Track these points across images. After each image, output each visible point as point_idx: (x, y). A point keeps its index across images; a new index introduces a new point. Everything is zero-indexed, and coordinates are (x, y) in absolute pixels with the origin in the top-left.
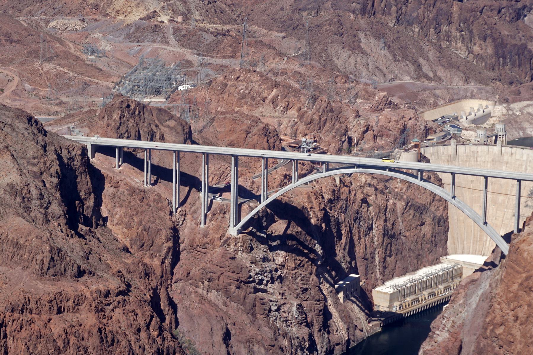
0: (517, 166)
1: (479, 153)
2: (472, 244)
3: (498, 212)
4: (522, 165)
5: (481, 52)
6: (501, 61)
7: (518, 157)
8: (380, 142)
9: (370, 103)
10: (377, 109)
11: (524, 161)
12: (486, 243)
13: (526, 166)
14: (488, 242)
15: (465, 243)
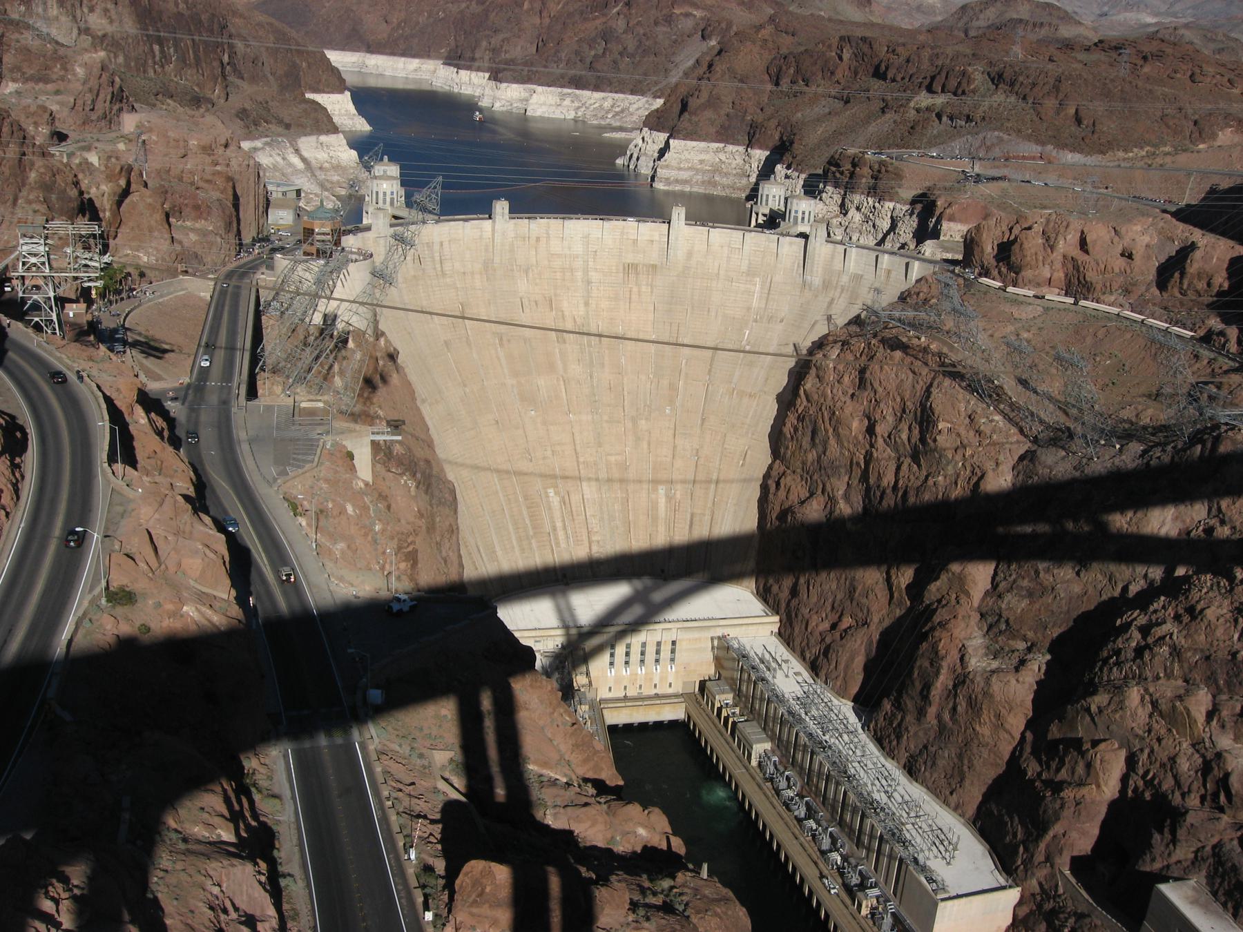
0: (559, 275)
1: (446, 245)
2: (517, 550)
4: (572, 270)
5: (110, 29)
6: (157, 53)
7: (556, 246)
8: (191, 231)
9: (57, 92)
10: (94, 117)
12: (556, 539)
13: (586, 271)
14: (561, 534)
15: (499, 553)
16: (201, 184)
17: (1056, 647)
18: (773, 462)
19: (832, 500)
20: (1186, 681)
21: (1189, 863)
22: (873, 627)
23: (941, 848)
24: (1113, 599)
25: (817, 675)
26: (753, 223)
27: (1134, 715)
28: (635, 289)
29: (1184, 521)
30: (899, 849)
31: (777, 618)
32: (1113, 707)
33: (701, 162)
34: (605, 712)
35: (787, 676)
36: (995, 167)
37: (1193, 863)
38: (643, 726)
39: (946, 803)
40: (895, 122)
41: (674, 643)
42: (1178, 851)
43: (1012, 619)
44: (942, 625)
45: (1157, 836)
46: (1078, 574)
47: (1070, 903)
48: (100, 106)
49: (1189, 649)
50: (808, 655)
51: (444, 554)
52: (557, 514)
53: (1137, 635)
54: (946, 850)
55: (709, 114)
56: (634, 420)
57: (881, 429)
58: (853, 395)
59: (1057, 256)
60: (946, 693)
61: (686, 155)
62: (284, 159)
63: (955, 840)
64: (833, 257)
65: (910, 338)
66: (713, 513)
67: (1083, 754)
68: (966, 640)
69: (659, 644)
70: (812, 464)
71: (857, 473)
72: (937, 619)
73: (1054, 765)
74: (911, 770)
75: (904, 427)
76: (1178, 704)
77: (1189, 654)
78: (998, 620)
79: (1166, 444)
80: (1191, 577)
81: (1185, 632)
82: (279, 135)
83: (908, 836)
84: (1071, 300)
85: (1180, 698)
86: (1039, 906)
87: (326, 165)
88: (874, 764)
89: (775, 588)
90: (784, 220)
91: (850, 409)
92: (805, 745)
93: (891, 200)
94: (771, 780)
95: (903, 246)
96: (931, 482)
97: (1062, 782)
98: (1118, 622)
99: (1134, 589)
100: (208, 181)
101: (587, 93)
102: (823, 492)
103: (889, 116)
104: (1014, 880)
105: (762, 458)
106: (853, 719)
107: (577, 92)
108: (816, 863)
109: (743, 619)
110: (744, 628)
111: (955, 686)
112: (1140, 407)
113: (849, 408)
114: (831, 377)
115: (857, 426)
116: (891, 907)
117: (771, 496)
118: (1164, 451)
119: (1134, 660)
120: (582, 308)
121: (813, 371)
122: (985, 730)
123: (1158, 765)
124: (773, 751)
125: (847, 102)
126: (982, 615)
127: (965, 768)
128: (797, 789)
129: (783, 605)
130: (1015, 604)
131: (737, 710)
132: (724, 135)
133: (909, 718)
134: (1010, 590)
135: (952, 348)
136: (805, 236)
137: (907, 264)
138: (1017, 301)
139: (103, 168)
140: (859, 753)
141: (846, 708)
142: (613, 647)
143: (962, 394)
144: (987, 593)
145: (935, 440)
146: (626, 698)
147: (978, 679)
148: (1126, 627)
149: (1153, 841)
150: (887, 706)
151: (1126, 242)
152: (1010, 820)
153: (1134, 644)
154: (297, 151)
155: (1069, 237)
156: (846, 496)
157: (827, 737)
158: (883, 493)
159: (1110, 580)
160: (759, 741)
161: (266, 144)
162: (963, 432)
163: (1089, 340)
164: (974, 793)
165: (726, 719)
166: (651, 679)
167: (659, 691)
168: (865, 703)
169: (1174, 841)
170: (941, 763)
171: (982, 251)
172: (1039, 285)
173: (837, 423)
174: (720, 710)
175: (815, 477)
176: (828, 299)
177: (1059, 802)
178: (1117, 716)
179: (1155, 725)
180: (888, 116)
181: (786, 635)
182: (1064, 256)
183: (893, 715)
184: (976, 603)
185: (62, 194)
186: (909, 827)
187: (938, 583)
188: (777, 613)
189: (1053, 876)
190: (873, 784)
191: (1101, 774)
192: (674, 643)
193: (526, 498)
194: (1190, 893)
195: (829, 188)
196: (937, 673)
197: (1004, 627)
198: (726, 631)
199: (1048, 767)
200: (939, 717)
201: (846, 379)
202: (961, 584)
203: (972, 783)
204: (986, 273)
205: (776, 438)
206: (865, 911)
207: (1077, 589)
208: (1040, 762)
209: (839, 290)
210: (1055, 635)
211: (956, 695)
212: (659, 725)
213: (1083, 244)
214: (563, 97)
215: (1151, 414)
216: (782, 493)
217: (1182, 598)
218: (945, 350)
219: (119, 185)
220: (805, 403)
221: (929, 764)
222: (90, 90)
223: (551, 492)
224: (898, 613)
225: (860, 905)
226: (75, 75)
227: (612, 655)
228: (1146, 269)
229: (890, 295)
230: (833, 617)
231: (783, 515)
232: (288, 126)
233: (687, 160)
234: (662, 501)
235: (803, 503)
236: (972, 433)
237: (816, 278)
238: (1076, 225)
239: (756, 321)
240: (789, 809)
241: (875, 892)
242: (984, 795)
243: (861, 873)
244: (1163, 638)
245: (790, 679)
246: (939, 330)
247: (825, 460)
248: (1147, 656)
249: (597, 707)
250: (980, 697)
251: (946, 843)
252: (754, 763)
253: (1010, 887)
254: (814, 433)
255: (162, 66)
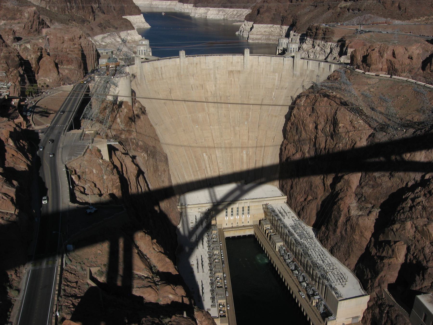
0: (205, 76)
3: (204, 131)
7: (203, 66)
9: (19, 23)
11: (211, 69)
12: (207, 171)
14: (208, 169)
16: (69, 52)
17: (382, 206)
18: (284, 140)
19: (304, 153)
20: (428, 219)
21: (429, 287)
22: (319, 199)
23: (341, 281)
24: (403, 188)
25: (300, 217)
26: (277, 53)
27: (409, 232)
28: (233, 80)
29: (428, 158)
30: (326, 282)
31: (286, 197)
32: (401, 229)
33: (265, 32)
34: (225, 232)
35: (289, 218)
36: (368, 27)
37: (431, 287)
38: (239, 237)
39: (344, 264)
40: (333, 13)
41: (249, 207)
42: (425, 283)
43: (366, 196)
44: (341, 199)
45: (417, 277)
46: (390, 179)
47: (387, 301)
48: (34, 27)
49: (429, 207)
50: (297, 210)
51: (162, 179)
52: (207, 162)
53: (410, 202)
54: (343, 282)
55: (267, 14)
56: (234, 127)
57: (320, 127)
58: (310, 115)
59: (384, 60)
60: (343, 224)
61: (259, 29)
62: (115, 40)
63: (346, 278)
64: (303, 64)
65: (330, 93)
66: (263, 160)
67: (391, 246)
68: (350, 204)
69: (243, 208)
70: (297, 140)
71: (312, 143)
72: (340, 197)
73: (381, 250)
74: (332, 252)
75: (328, 126)
76: (425, 228)
77: (429, 209)
78: (362, 197)
79: (422, 129)
80: (430, 179)
81: (427, 200)
82: (114, 32)
83: (330, 277)
84: (389, 76)
85: (425, 225)
86: (376, 302)
87: (130, 41)
88: (319, 250)
89: (285, 186)
90: (287, 51)
91: (309, 120)
92: (294, 244)
93: (330, 42)
94: (283, 256)
95: (334, 59)
96: (337, 146)
97: (384, 257)
98: (404, 197)
99: (410, 184)
100: (72, 51)
101: (228, 9)
102: (301, 151)
103: (331, 11)
104: (367, 292)
105: (280, 139)
106: (312, 233)
107: (224, 9)
108: (297, 286)
109: (274, 197)
110: (274, 201)
111: (346, 221)
112: (414, 115)
113: (308, 120)
114: (303, 109)
115: (311, 126)
116: (323, 302)
117: (283, 153)
118: (421, 132)
119: (409, 211)
120: (214, 88)
121: (296, 107)
122: (357, 237)
123: (418, 250)
124: (284, 245)
125: (316, 7)
126: (356, 195)
127: (350, 251)
128: (291, 259)
129: (288, 192)
130: (367, 191)
131: (272, 231)
132: (273, 21)
133: (330, 233)
134: (366, 185)
135: (344, 96)
136: (293, 57)
137: (330, 66)
138: (369, 77)
139: (32, 49)
140: (313, 246)
141: (310, 230)
142: (227, 209)
143: (348, 113)
144: (358, 187)
145: (338, 131)
146: (232, 227)
147: (354, 218)
148: (406, 198)
149: (416, 279)
150: (323, 228)
151: (410, 53)
152: (366, 270)
153: (409, 205)
154: (120, 37)
155: (388, 52)
156: (309, 152)
157: (302, 240)
158: (321, 150)
159: (401, 181)
160: (278, 242)
161: (109, 35)
162: (348, 127)
163: (396, 91)
164: (354, 260)
165: (268, 234)
166: (241, 220)
167: (244, 224)
168: (316, 228)
169: (424, 279)
170: (341, 249)
171: (357, 59)
172: (378, 71)
173: (304, 125)
174: (265, 230)
175: (298, 145)
176: (302, 80)
177: (382, 264)
178: (403, 232)
179: (417, 236)
180: (330, 11)
181: (289, 203)
182: (387, 60)
183: (325, 232)
184: (354, 190)
185: (13, 60)
186: (330, 273)
187: (340, 183)
188: (286, 195)
189: (380, 291)
190: (318, 257)
191: (397, 254)
192: (249, 207)
193: (195, 157)
194: (429, 299)
195: (308, 39)
196: (340, 217)
197: (364, 199)
198: (267, 202)
199: (379, 251)
200: (341, 232)
201: (308, 109)
202: (348, 182)
203: (353, 257)
204: (358, 67)
205: (284, 131)
206: (314, 304)
207: (390, 184)
208: (376, 249)
209: (306, 76)
210: (382, 202)
211: (346, 225)
212: (244, 237)
213: (394, 54)
214: (219, 11)
215: (418, 118)
216: (287, 152)
217: (427, 187)
218: (342, 97)
219: (37, 55)
220: (294, 118)
221: (338, 250)
222: (30, 21)
223: (205, 154)
224: (327, 194)
225: (312, 302)
226: (24, 16)
227: (227, 212)
228: (418, 63)
229: (323, 77)
230: (305, 196)
231: (288, 159)
232: (116, 28)
233: (260, 31)
234: (245, 156)
235: (294, 155)
236: (351, 127)
237: (298, 72)
238: (391, 48)
239: (277, 89)
240: (289, 267)
241: (318, 297)
242: (358, 261)
243: (313, 290)
244: (419, 203)
245: (290, 219)
246: (340, 89)
247: (301, 139)
248: (413, 210)
249: (221, 231)
250: (355, 225)
251: (343, 279)
252: (277, 250)
253: (366, 295)
254: (297, 129)
255: (71, 10)
